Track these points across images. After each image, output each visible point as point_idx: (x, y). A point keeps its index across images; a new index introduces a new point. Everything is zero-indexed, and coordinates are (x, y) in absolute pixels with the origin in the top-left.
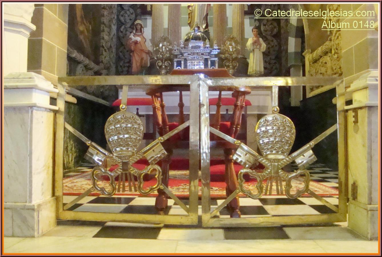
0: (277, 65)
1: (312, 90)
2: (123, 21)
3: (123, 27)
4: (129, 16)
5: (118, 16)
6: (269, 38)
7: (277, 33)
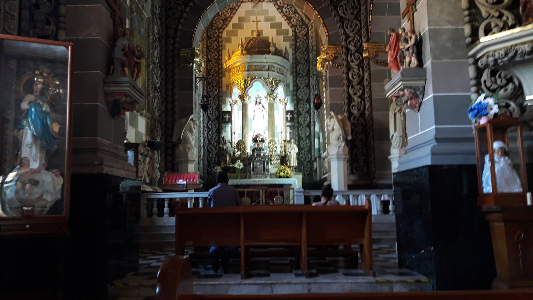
0: (309, 155)
1: (324, 174)
2: (211, 128)
3: (211, 132)
4: (214, 125)
6: (304, 138)
7: (309, 135)
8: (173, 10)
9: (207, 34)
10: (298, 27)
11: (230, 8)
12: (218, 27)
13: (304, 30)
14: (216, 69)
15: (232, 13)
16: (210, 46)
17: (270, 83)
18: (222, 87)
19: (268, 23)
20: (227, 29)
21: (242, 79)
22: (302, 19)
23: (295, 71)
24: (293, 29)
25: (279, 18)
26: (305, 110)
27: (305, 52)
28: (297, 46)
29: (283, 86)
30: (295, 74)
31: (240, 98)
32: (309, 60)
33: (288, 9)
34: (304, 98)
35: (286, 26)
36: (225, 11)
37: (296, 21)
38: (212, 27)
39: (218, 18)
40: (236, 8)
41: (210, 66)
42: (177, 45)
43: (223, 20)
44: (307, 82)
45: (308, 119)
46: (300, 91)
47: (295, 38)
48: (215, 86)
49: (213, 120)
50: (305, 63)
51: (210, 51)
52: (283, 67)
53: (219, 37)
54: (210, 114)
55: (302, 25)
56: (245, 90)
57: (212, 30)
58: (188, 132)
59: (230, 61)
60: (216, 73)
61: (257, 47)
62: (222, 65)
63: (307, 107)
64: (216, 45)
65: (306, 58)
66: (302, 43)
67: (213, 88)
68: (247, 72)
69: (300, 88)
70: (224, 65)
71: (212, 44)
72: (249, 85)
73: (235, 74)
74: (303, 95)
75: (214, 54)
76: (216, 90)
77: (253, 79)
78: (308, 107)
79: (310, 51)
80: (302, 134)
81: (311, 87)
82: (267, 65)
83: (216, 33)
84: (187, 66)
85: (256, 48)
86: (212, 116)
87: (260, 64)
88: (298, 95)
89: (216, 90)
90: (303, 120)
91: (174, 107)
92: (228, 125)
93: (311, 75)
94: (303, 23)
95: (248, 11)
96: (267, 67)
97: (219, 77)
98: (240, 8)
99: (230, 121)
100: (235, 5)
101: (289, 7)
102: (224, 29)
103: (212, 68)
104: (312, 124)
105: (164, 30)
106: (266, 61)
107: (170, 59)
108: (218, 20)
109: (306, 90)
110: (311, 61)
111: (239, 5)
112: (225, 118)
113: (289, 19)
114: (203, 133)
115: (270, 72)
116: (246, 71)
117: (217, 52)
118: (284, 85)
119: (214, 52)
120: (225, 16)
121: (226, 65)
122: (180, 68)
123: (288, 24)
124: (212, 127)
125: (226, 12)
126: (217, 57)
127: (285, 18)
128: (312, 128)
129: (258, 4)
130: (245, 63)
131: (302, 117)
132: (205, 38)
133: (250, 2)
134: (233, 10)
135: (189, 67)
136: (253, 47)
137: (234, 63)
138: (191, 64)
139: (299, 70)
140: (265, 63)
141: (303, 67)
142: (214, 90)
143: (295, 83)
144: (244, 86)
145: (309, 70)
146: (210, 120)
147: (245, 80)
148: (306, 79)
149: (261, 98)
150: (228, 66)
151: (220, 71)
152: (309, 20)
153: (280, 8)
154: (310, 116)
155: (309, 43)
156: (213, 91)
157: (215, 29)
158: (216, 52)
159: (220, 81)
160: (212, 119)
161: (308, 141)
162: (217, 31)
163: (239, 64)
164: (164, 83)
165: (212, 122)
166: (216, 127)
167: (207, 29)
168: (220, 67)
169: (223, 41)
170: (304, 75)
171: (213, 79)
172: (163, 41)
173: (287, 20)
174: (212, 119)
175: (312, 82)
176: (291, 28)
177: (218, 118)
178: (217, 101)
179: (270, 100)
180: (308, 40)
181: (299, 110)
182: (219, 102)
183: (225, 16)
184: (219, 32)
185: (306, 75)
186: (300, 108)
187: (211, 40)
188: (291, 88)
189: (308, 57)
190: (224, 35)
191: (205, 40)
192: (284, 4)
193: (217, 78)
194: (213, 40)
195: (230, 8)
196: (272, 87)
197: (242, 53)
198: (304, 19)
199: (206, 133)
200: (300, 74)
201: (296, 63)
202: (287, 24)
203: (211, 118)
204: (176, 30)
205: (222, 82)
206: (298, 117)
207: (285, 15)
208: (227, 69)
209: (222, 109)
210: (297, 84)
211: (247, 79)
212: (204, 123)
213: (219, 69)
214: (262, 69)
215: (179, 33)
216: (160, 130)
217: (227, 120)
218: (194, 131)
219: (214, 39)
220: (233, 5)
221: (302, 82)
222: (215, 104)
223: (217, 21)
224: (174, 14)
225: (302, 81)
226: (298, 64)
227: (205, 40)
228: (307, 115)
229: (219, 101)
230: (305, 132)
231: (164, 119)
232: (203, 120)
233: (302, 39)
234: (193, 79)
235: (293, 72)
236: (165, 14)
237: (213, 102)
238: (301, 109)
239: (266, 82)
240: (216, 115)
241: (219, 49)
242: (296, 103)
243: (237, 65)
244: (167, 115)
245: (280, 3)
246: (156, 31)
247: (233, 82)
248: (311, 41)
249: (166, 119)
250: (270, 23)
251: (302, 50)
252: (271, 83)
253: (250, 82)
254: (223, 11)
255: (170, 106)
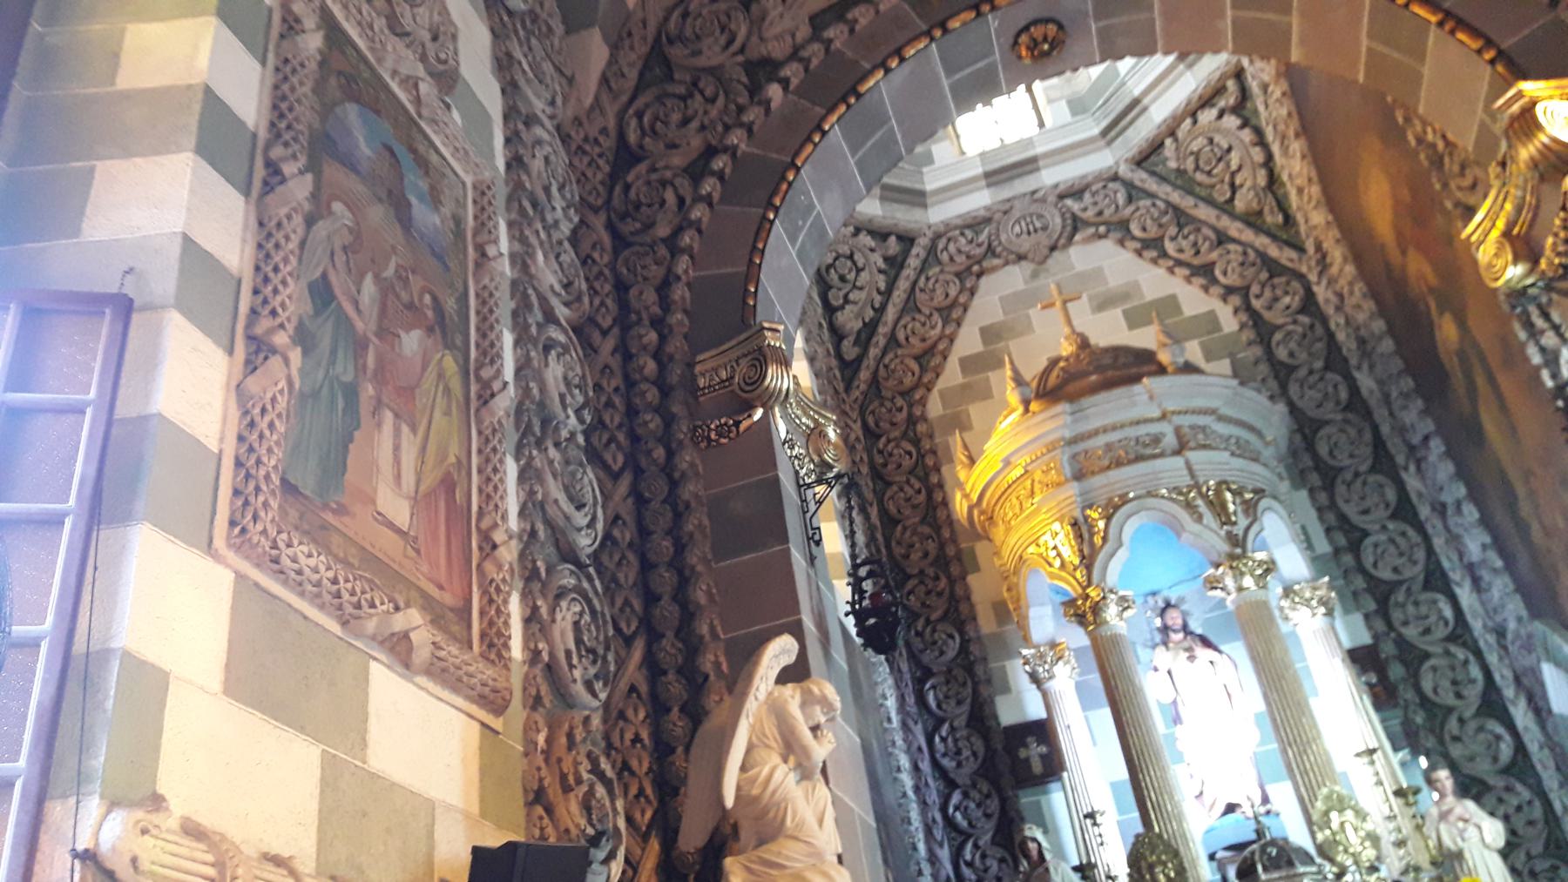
2: (964, 824)
3: (969, 846)
4: (979, 805)
5: (944, 809)
6: (1498, 782)
8: (644, 209)
9: (865, 426)
10: (1255, 289)
11: (939, 310)
12: (901, 388)
13: (1287, 293)
14: (931, 546)
15: (946, 322)
16: (885, 465)
17: (1210, 504)
18: (974, 619)
19: (1117, 313)
20: (941, 384)
21: (1056, 526)
22: (1262, 255)
23: (1310, 463)
24: (1236, 300)
25: (1155, 281)
26: (1441, 632)
27: (1329, 376)
28: (1281, 363)
29: (1276, 512)
30: (1315, 479)
31: (1076, 615)
32: (1364, 402)
33: (1185, 237)
34: (1407, 574)
35: (1194, 300)
36: (918, 325)
37: (1238, 270)
38: (880, 391)
39: (896, 357)
40: (962, 299)
41: (899, 543)
42: (676, 345)
43: (917, 358)
44: (1391, 495)
45: (1475, 671)
46: (1376, 545)
47: (1259, 334)
48: (943, 619)
49: (968, 782)
50: (1346, 421)
51: (889, 484)
52: (1251, 429)
53: (912, 421)
54: (944, 755)
55: (1271, 277)
56: (1089, 568)
57: (882, 405)
58: (776, 759)
59: (980, 466)
60: (932, 565)
61: (1091, 368)
62: (945, 503)
63: (1440, 611)
64: (910, 454)
65: (1344, 395)
66: (1299, 345)
67: (934, 631)
68: (1073, 489)
69: (1365, 534)
70: (958, 496)
71: (891, 455)
72: (1105, 539)
73: (1016, 516)
74: (1399, 562)
75: (907, 488)
76: (951, 636)
77: (1117, 508)
78: (1448, 613)
79: (1353, 361)
80: (1472, 759)
81: (1424, 512)
82: (1166, 429)
83: (900, 410)
84: (737, 424)
85: (1086, 374)
86: (959, 765)
87: (1132, 432)
88: (1368, 560)
89: (951, 636)
90: (1446, 684)
91: (693, 649)
92: (1046, 793)
93: (1400, 459)
94: (1273, 268)
95: (1016, 295)
96: (1170, 440)
97: (949, 577)
98: (976, 297)
99: (1053, 767)
100: (953, 292)
101: (1186, 231)
102: (929, 390)
103: (912, 546)
104: (1509, 692)
105: (609, 302)
106: (1157, 414)
107: (648, 417)
108: (897, 361)
109: (1403, 534)
110: (1373, 402)
111: (968, 285)
112: (1027, 760)
113: (1204, 273)
114: (933, 859)
115: (1193, 456)
116: (1067, 481)
117: (919, 479)
118: (1283, 513)
119: (908, 482)
120: (923, 340)
121: (966, 496)
122: (703, 445)
123: (1206, 289)
124: (970, 824)
125: (924, 324)
126: (922, 498)
127: (1182, 272)
128: (1521, 714)
129: (1050, 262)
130: (1051, 447)
131: (1434, 669)
132: (857, 439)
133: (1014, 262)
134: (952, 313)
135: (749, 428)
136: (1070, 377)
137: (1000, 465)
138: (758, 414)
139: (1331, 453)
140: (1151, 420)
141: (1343, 438)
142: (940, 636)
143: (1331, 518)
144: (1081, 551)
145: (1379, 444)
146: (951, 784)
147: (1075, 524)
148: (1381, 486)
149: (1184, 607)
150: (975, 497)
151: (950, 551)
152: (1301, 249)
153: (1152, 247)
154: (1478, 654)
155: (1331, 336)
156: (935, 643)
157: (894, 397)
158: (913, 480)
159: (959, 591)
160: (959, 781)
161: (1526, 794)
162: (900, 402)
163: (1023, 460)
164: (625, 535)
165: (966, 795)
166: (988, 816)
167: (861, 407)
168: (946, 534)
169: (937, 434)
170: (1363, 468)
171: (928, 593)
172: (609, 344)
173: (1194, 279)
174: (962, 777)
175: (1423, 490)
176: (1224, 299)
177: (988, 770)
178: (964, 684)
179: (1240, 589)
180: (1324, 321)
181: (1400, 635)
182: (975, 692)
183: (923, 340)
184: (910, 406)
185: (1373, 469)
186: (1406, 623)
187: (883, 440)
188: (1323, 546)
189: (1354, 389)
190: (935, 407)
191: (859, 447)
192: (1160, 226)
193: (943, 583)
194: (895, 439)
195: (939, 310)
196: (1229, 522)
197: (1027, 410)
198: (1273, 251)
199: (944, 854)
200: (1341, 469)
201: (1305, 428)
202: (1202, 294)
203: (952, 775)
204: (664, 287)
205: (968, 598)
206: (1414, 678)
207: (1179, 263)
208: (976, 512)
209: (995, 717)
210: (1343, 518)
211: (1086, 518)
212: (924, 804)
213: (942, 546)
214: (1149, 451)
215: (679, 292)
216: (620, 804)
217: (1037, 768)
218: (821, 751)
219: (896, 434)
220: (947, 295)
221: (1368, 503)
222: (959, 703)
223: (892, 366)
224: (649, 226)
225: (1363, 498)
226: (1316, 431)
227: (859, 447)
228: (1460, 653)
229: (975, 685)
230: (1489, 746)
231: (645, 735)
232: (917, 789)
233: (1291, 327)
234: (776, 481)
235: (1302, 472)
236: (607, 240)
237: (947, 697)
238: (1411, 633)
239: (1189, 506)
240: (974, 754)
241: (925, 466)
242: (1372, 606)
243: (1019, 471)
244: (658, 708)
245: (1144, 229)
246: (548, 275)
247: (1021, 557)
248: (1342, 321)
249: (656, 735)
250: (1125, 313)
251: (1311, 372)
252: (1219, 508)
253: (1101, 524)
254: (910, 326)
255: (670, 648)
